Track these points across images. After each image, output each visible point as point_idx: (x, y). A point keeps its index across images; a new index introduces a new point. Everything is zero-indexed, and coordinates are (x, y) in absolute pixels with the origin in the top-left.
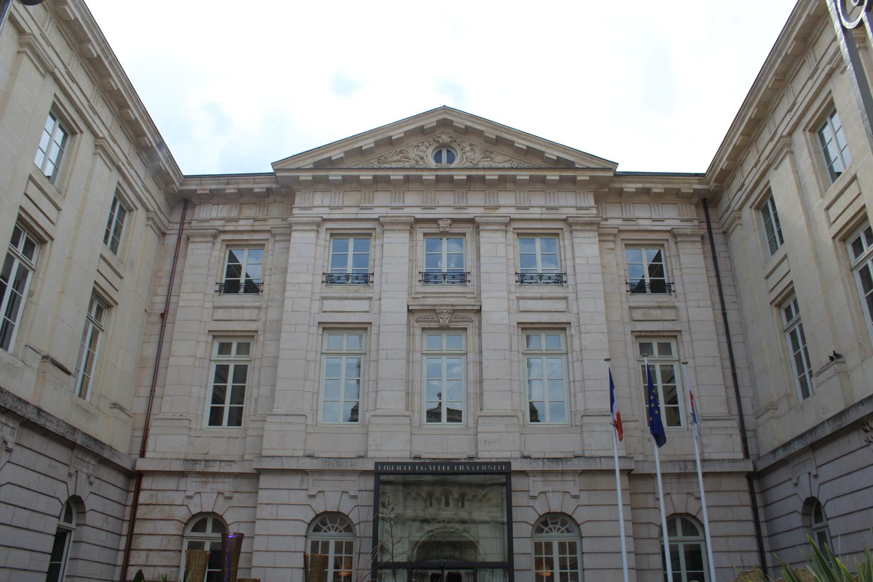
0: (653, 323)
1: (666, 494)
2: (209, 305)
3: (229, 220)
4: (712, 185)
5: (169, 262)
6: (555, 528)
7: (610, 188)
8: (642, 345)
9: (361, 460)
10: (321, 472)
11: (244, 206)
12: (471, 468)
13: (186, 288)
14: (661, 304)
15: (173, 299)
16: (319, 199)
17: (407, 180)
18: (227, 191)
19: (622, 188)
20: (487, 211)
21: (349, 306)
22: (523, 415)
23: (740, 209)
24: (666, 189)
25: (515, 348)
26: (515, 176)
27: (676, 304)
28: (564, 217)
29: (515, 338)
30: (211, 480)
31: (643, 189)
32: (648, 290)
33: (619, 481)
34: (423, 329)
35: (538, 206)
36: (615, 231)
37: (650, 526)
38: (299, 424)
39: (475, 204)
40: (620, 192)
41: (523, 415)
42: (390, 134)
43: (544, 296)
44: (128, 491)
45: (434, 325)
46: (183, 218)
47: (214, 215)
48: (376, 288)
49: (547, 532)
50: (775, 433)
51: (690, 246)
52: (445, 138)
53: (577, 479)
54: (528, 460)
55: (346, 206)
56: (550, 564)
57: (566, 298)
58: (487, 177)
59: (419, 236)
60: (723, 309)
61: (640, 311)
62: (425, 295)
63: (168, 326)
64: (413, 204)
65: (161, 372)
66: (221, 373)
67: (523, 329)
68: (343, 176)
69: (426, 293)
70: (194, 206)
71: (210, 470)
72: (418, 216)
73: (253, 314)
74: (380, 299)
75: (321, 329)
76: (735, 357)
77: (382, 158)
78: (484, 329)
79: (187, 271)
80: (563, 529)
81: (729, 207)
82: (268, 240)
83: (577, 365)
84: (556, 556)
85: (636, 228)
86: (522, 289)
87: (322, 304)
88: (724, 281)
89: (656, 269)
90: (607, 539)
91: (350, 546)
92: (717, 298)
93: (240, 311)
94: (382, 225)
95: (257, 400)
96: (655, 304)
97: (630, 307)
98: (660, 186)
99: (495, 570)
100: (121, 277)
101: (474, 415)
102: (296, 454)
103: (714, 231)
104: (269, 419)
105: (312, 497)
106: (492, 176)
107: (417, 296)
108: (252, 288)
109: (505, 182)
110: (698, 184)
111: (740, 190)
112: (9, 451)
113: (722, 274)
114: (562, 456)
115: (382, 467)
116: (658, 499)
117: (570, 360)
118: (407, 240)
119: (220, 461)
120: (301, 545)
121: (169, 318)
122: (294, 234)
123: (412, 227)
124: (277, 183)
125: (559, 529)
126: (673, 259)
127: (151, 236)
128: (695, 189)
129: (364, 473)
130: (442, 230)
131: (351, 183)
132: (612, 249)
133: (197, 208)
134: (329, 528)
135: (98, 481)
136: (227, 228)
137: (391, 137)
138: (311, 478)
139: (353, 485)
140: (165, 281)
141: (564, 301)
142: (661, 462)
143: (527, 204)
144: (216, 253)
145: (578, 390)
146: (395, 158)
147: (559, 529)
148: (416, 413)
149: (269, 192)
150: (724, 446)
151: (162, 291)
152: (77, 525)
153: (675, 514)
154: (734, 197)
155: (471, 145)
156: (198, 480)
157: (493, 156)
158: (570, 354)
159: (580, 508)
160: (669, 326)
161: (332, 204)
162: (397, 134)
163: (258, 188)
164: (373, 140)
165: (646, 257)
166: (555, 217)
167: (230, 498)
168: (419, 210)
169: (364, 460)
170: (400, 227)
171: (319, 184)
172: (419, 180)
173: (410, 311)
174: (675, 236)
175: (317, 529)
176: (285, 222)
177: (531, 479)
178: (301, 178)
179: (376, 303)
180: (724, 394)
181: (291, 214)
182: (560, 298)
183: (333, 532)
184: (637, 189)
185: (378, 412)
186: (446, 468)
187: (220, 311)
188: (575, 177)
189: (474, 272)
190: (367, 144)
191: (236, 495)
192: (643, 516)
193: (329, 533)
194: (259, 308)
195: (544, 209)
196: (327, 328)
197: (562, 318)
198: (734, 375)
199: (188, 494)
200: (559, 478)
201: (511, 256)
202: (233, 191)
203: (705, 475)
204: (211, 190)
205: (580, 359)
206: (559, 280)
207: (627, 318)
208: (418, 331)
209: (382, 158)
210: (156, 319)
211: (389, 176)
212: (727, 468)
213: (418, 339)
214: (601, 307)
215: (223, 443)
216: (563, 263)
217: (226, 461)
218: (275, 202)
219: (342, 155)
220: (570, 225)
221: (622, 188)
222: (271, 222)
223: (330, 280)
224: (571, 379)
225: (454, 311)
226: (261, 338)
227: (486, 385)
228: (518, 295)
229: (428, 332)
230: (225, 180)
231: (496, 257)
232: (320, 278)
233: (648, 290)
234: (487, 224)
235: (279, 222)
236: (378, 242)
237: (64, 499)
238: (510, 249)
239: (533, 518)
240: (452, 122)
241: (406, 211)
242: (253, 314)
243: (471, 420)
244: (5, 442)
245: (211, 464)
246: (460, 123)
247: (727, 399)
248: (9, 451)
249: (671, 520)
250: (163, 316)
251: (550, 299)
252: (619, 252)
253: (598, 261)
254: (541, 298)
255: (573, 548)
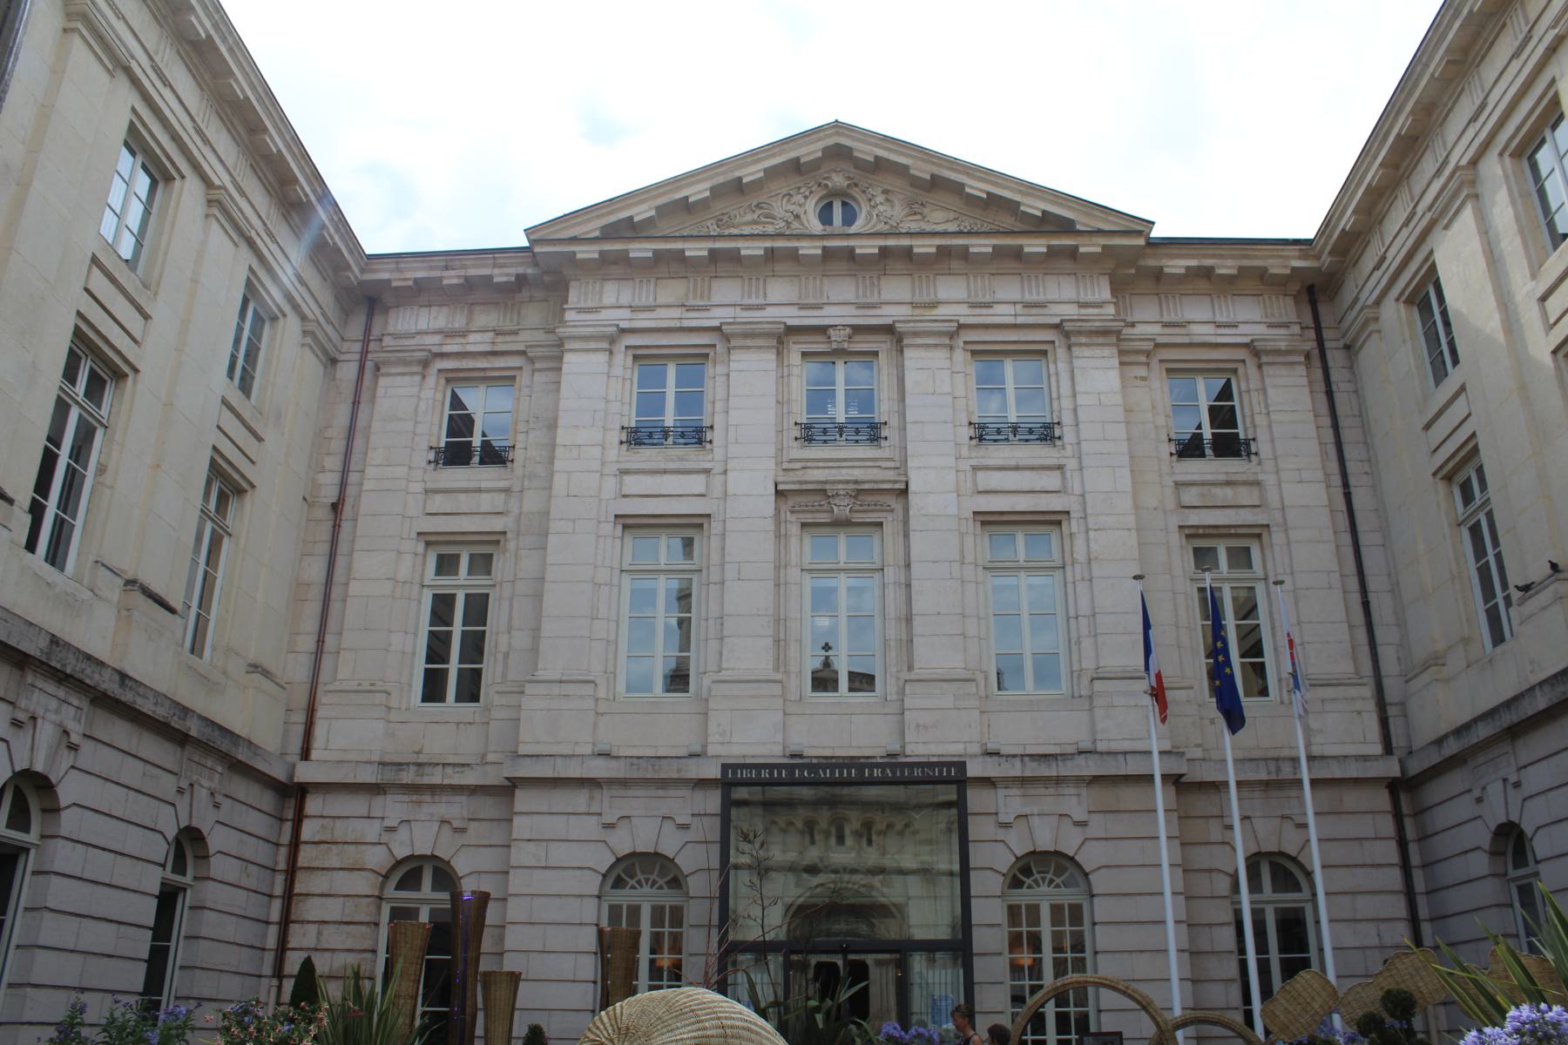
0: (1218, 512)
1: (1244, 818)
2: (417, 487)
3: (449, 334)
4: (1326, 260)
5: (343, 411)
6: (1044, 879)
7: (1139, 268)
8: (1197, 551)
9: (695, 760)
10: (624, 783)
11: (477, 308)
12: (894, 773)
13: (376, 457)
14: (1234, 478)
15: (353, 478)
16: (611, 293)
17: (771, 254)
18: (445, 282)
19: (1161, 268)
20: (917, 311)
21: (669, 485)
22: (986, 679)
23: (1378, 302)
24: (1240, 269)
25: (969, 558)
26: (967, 247)
27: (1260, 477)
28: (1056, 320)
29: (969, 540)
30: (427, 798)
31: (1199, 268)
32: (1208, 451)
33: (1160, 795)
34: (804, 525)
35: (1006, 299)
36: (1148, 346)
37: (1214, 875)
38: (582, 697)
39: (894, 299)
40: (1158, 275)
41: (986, 679)
42: (737, 174)
43: (1022, 463)
44: (282, 820)
45: (823, 518)
46: (368, 330)
47: (422, 325)
48: (718, 452)
49: (1029, 887)
50: (1444, 706)
51: (1284, 371)
52: (839, 181)
53: (1084, 791)
54: (995, 758)
55: (663, 306)
56: (1035, 943)
57: (1060, 468)
58: (916, 250)
59: (795, 358)
60: (1346, 484)
61: (1194, 490)
62: (807, 464)
63: (346, 527)
64: (781, 301)
65: (335, 607)
66: (442, 607)
67: (983, 523)
68: (655, 252)
69: (808, 460)
70: (386, 310)
71: (426, 780)
72: (791, 322)
73: (498, 501)
74: (725, 472)
75: (620, 528)
76: (1367, 571)
77: (725, 218)
78: (913, 524)
79: (376, 426)
80: (1058, 881)
81: (1356, 300)
82: (520, 368)
83: (1082, 588)
84: (1046, 930)
85: (1186, 340)
86: (982, 451)
87: (621, 483)
88: (1346, 435)
89: (1223, 415)
90: (1139, 898)
91: (677, 916)
92: (1334, 466)
93: (473, 497)
94: (727, 338)
95: (506, 655)
96: (1222, 478)
97: (1177, 484)
98: (1230, 262)
99: (938, 955)
100: (260, 439)
101: (898, 679)
102: (578, 751)
103: (1327, 345)
104: (529, 689)
105: (610, 826)
106: (925, 247)
107: (792, 466)
108: (494, 456)
109: (948, 259)
110: (1300, 258)
111: (1377, 268)
112: (73, 748)
113: (1344, 422)
114: (1057, 750)
115: (735, 773)
116: (1230, 827)
117: (1070, 579)
118: (773, 365)
119: (444, 765)
120: (590, 911)
121: (347, 510)
122: (568, 357)
123: (780, 342)
124: (536, 265)
125: (1051, 881)
126: (1254, 395)
127: (311, 364)
128: (1293, 269)
129: (702, 783)
130: (834, 346)
131: (669, 264)
132: (1143, 379)
133: (392, 314)
134: (639, 882)
135: (229, 801)
136: (446, 349)
137: (740, 179)
138: (606, 793)
139: (683, 805)
140: (338, 445)
141: (1057, 473)
142: (1235, 761)
143: (988, 299)
144: (427, 394)
145: (1084, 631)
146: (749, 217)
147: (1051, 881)
148: (793, 677)
149: (521, 280)
150: (1348, 732)
151: (333, 463)
152: (196, 878)
153: (1258, 854)
154: (1366, 281)
155: (885, 192)
156: (405, 798)
157: (926, 211)
158: (1068, 568)
159: (1088, 844)
161: (636, 303)
162: (750, 174)
163: (501, 276)
164: (708, 185)
165: (1204, 393)
166: (1041, 320)
167: (463, 830)
168: (793, 311)
169: (701, 760)
170: (759, 342)
171: (613, 266)
172: (793, 256)
173: (779, 493)
174: (1257, 354)
175: (619, 883)
176: (551, 336)
177: (1001, 792)
178: (579, 256)
179: (717, 480)
180: (1347, 638)
181: (562, 322)
182: (1049, 468)
183: (646, 889)
184: (1188, 268)
185: (724, 675)
186: (849, 773)
187: (438, 497)
188: (1076, 247)
189: (894, 421)
190: (698, 192)
191: (473, 826)
192: (1202, 857)
193: (640, 891)
194: (507, 491)
195: (1019, 307)
196: (630, 524)
197: (1055, 503)
198: (1366, 605)
199: (388, 823)
200: (1052, 791)
201: (960, 392)
202: (455, 281)
203: (1314, 783)
204: (416, 280)
205: (1087, 577)
206: (1047, 434)
207: (1170, 503)
208: (795, 529)
209: (725, 218)
210: (324, 513)
211: (738, 249)
212: (1353, 771)
213: (794, 542)
214: (1125, 483)
215: (447, 734)
216: (1055, 404)
217: (454, 765)
218: (531, 299)
219: (653, 213)
220: (1067, 335)
221: (1161, 268)
222: (525, 336)
223: (636, 438)
224: (1072, 614)
225: (859, 492)
226: (511, 545)
227: (919, 625)
228: (974, 462)
229: (815, 531)
230: (441, 262)
231: (933, 394)
232: (616, 436)
233: (1208, 451)
234: (916, 334)
235: (540, 336)
236: (720, 369)
237: (171, 833)
238: (959, 378)
239: (1005, 862)
240: (850, 149)
241: (770, 313)
242: (498, 501)
243: (892, 689)
244: (66, 733)
245: (428, 770)
246: (865, 152)
247: (1353, 647)
248: (73, 748)
249: (1253, 863)
250: (336, 507)
251: (1033, 468)
252: (1156, 384)
253: (1118, 399)
254: (1017, 468)
255: (1076, 913)
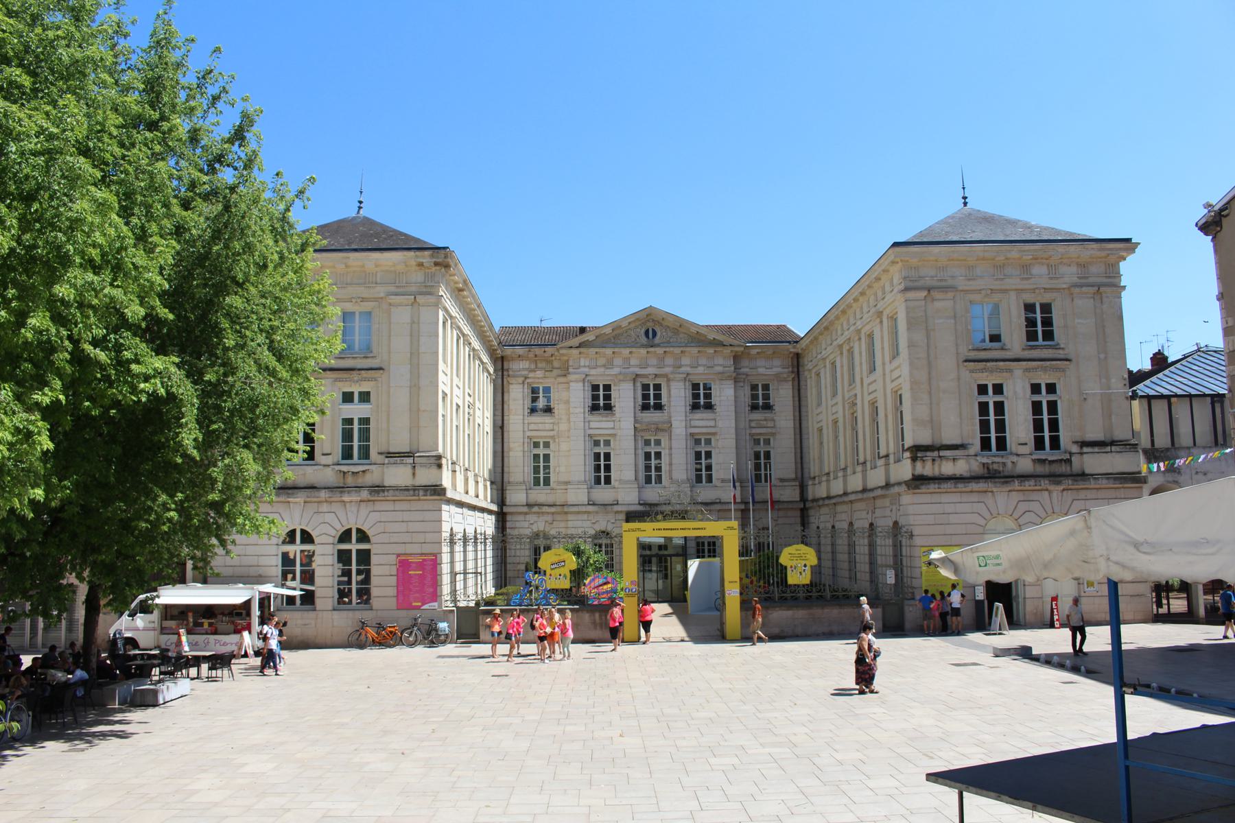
129: (617, 512)
160: (770, 430)
197: (712, 430)
212: (790, 506)
250: (502, 427)
